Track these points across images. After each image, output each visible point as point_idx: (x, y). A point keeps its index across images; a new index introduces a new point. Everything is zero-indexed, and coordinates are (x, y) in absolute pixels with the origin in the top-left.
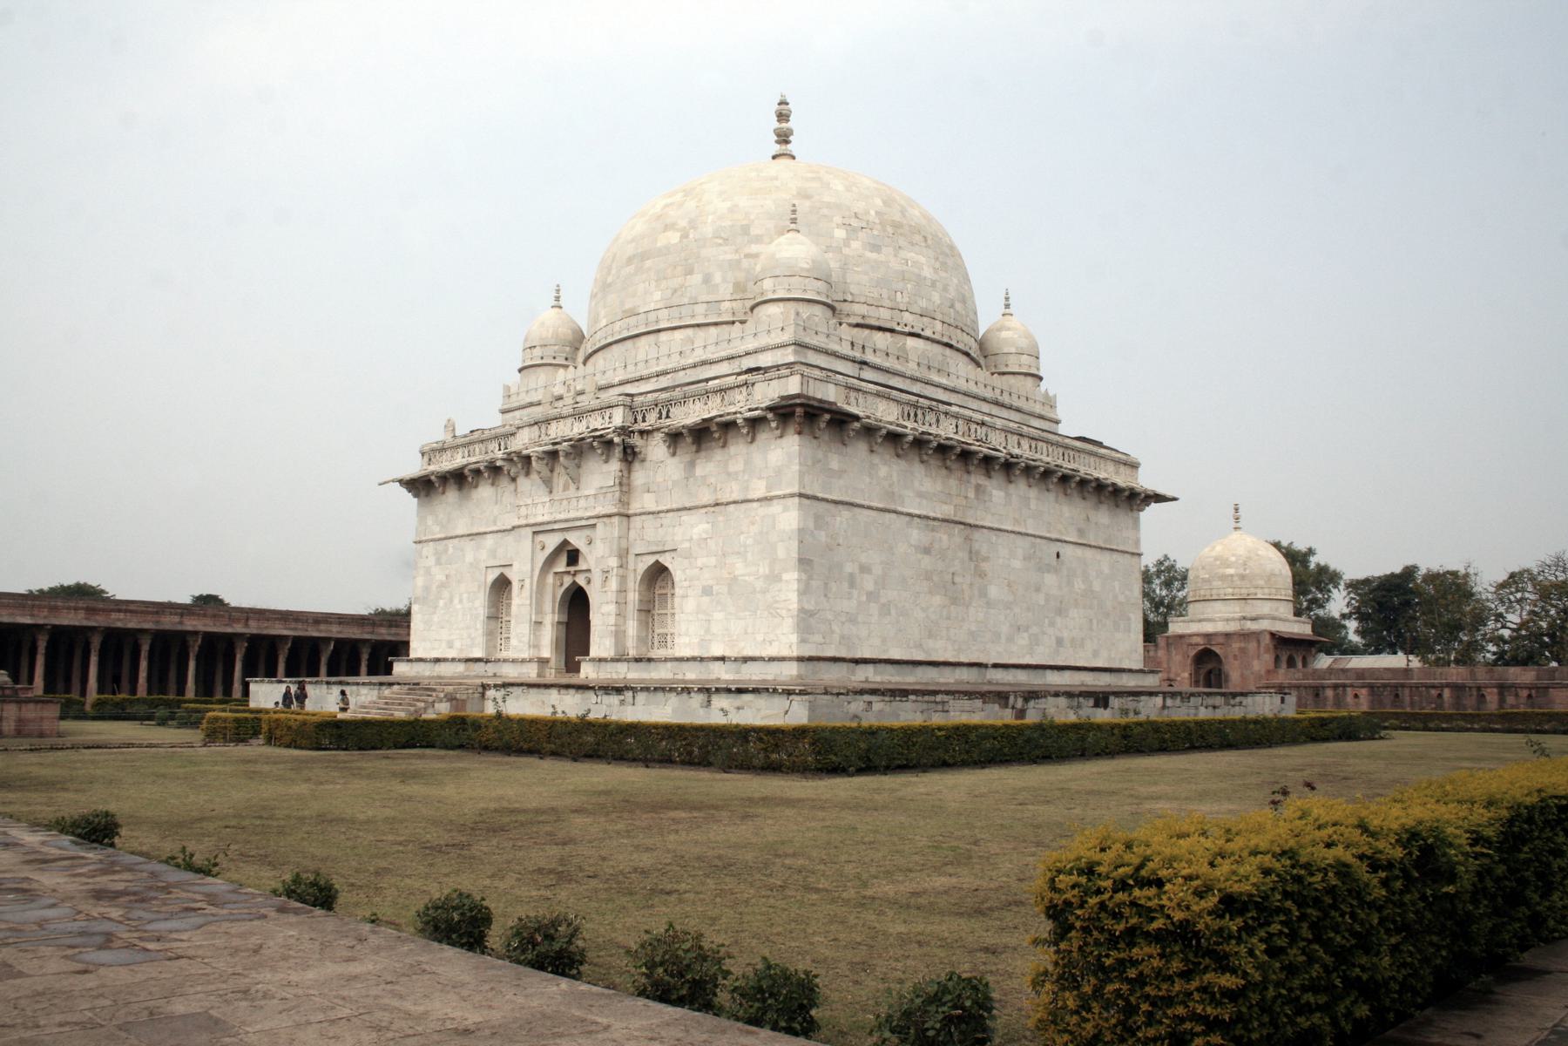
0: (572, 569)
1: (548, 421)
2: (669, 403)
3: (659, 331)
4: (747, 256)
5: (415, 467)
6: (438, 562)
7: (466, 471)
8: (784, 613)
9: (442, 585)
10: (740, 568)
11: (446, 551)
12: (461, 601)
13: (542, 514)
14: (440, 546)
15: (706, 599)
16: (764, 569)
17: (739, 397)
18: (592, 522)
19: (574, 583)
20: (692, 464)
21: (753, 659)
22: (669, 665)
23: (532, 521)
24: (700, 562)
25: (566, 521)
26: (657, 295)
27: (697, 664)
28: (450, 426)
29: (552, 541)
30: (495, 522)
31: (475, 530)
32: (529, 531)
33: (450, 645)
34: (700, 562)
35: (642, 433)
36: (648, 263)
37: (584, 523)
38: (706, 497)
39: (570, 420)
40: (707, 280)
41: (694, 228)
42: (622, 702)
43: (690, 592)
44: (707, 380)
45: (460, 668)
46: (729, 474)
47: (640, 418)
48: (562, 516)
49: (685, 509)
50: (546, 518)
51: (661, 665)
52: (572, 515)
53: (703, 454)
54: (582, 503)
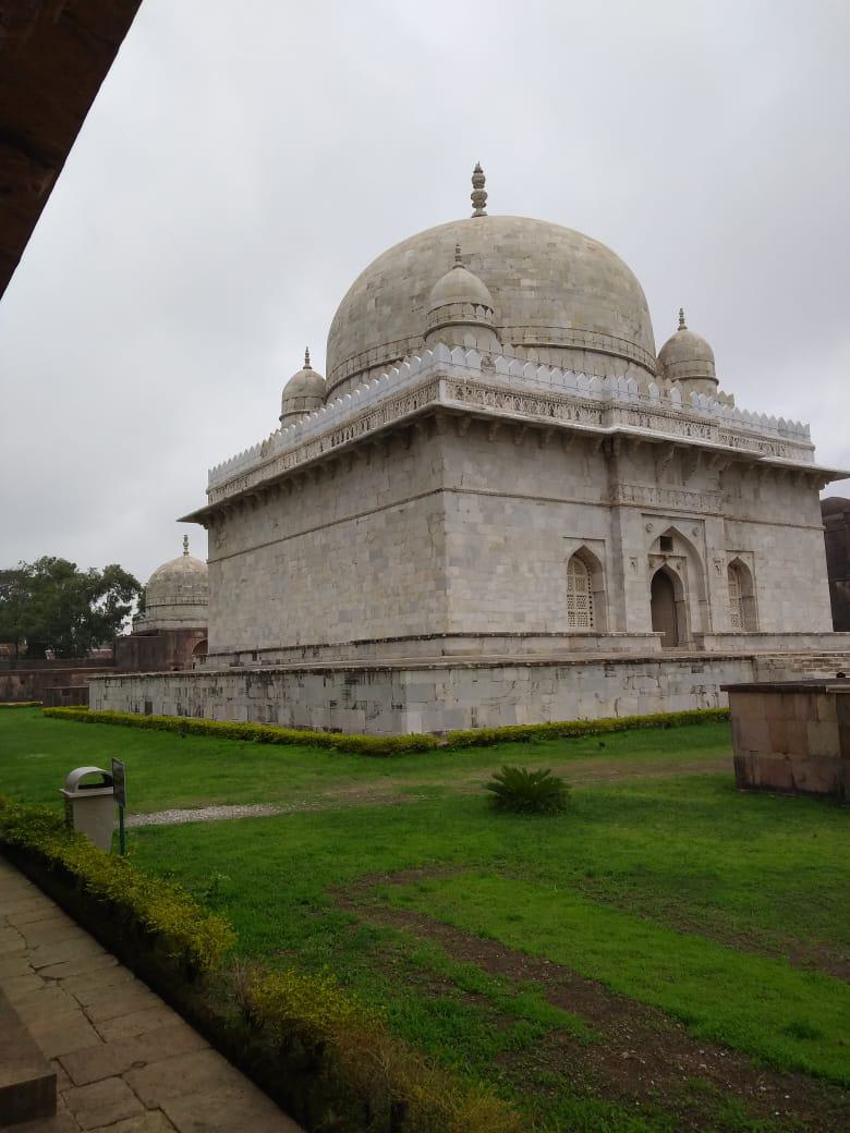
0: (667, 554)
6: (488, 520)
9: (497, 548)
12: (531, 570)
13: (651, 499)
18: (703, 517)
22: (775, 638)
33: (520, 618)
36: (613, 296)
45: (564, 643)
50: (655, 504)
51: (772, 639)
52: (680, 506)
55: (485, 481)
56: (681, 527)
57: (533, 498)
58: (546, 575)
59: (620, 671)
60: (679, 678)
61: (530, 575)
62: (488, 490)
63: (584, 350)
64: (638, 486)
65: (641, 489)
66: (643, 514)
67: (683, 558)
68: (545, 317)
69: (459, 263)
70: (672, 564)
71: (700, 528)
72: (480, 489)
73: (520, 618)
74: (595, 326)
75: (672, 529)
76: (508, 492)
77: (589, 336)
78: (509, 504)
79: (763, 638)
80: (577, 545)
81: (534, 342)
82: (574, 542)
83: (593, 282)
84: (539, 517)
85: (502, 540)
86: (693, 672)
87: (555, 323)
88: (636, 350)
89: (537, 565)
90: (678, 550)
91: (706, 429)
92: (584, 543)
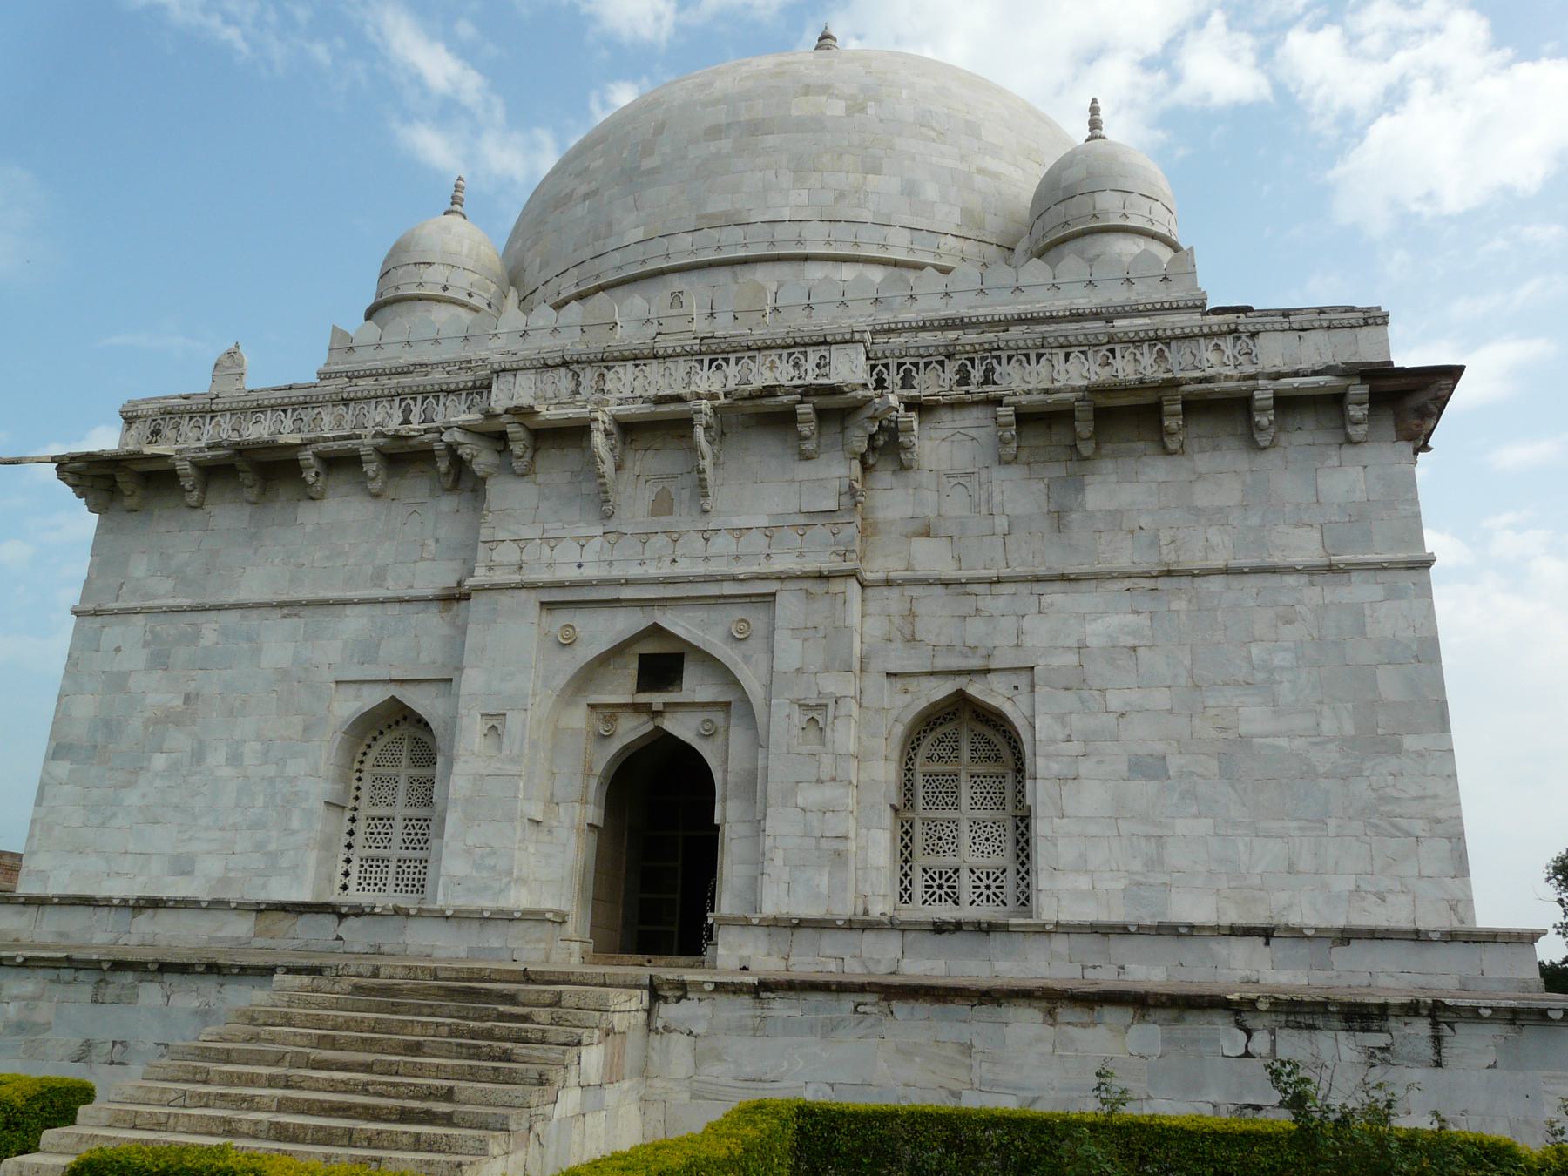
0: (657, 699)
2: (994, 352)
3: (807, 258)
4: (980, 171)
6: (159, 661)
7: (307, 456)
8: (1419, 827)
9: (168, 719)
10: (1253, 718)
11: (197, 636)
12: (234, 759)
14: (170, 628)
15: (1142, 791)
16: (1338, 722)
17: (1213, 357)
19: (658, 728)
20: (1076, 484)
21: (1374, 935)
23: (544, 576)
24: (1115, 701)
27: (1167, 944)
28: (229, 364)
30: (378, 578)
31: (305, 594)
32: (534, 598)
34: (1115, 701)
35: (911, 405)
36: (771, 141)
37: (729, 589)
38: (1125, 557)
39: (681, 366)
40: (910, 190)
41: (879, 101)
42: (1379, 1057)
43: (1085, 767)
45: (241, 927)
46: (1197, 512)
47: (893, 378)
48: (652, 571)
50: (591, 572)
52: (682, 568)
53: (1107, 465)
54: (721, 543)
55: (169, 584)
56: (681, 624)
58: (271, 770)
61: (226, 772)
62: (172, 602)
64: (536, 530)
65: (553, 542)
66: (544, 605)
67: (727, 705)
68: (597, 238)
69: (457, 207)
70: (682, 727)
71: (756, 617)
73: (183, 866)
74: (699, 217)
75: (656, 631)
78: (210, 629)
79: (997, 939)
80: (374, 698)
82: (366, 689)
84: (279, 644)
85: (178, 702)
87: (613, 243)
88: (838, 231)
89: (251, 749)
90: (695, 686)
91: (813, 356)
92: (394, 691)
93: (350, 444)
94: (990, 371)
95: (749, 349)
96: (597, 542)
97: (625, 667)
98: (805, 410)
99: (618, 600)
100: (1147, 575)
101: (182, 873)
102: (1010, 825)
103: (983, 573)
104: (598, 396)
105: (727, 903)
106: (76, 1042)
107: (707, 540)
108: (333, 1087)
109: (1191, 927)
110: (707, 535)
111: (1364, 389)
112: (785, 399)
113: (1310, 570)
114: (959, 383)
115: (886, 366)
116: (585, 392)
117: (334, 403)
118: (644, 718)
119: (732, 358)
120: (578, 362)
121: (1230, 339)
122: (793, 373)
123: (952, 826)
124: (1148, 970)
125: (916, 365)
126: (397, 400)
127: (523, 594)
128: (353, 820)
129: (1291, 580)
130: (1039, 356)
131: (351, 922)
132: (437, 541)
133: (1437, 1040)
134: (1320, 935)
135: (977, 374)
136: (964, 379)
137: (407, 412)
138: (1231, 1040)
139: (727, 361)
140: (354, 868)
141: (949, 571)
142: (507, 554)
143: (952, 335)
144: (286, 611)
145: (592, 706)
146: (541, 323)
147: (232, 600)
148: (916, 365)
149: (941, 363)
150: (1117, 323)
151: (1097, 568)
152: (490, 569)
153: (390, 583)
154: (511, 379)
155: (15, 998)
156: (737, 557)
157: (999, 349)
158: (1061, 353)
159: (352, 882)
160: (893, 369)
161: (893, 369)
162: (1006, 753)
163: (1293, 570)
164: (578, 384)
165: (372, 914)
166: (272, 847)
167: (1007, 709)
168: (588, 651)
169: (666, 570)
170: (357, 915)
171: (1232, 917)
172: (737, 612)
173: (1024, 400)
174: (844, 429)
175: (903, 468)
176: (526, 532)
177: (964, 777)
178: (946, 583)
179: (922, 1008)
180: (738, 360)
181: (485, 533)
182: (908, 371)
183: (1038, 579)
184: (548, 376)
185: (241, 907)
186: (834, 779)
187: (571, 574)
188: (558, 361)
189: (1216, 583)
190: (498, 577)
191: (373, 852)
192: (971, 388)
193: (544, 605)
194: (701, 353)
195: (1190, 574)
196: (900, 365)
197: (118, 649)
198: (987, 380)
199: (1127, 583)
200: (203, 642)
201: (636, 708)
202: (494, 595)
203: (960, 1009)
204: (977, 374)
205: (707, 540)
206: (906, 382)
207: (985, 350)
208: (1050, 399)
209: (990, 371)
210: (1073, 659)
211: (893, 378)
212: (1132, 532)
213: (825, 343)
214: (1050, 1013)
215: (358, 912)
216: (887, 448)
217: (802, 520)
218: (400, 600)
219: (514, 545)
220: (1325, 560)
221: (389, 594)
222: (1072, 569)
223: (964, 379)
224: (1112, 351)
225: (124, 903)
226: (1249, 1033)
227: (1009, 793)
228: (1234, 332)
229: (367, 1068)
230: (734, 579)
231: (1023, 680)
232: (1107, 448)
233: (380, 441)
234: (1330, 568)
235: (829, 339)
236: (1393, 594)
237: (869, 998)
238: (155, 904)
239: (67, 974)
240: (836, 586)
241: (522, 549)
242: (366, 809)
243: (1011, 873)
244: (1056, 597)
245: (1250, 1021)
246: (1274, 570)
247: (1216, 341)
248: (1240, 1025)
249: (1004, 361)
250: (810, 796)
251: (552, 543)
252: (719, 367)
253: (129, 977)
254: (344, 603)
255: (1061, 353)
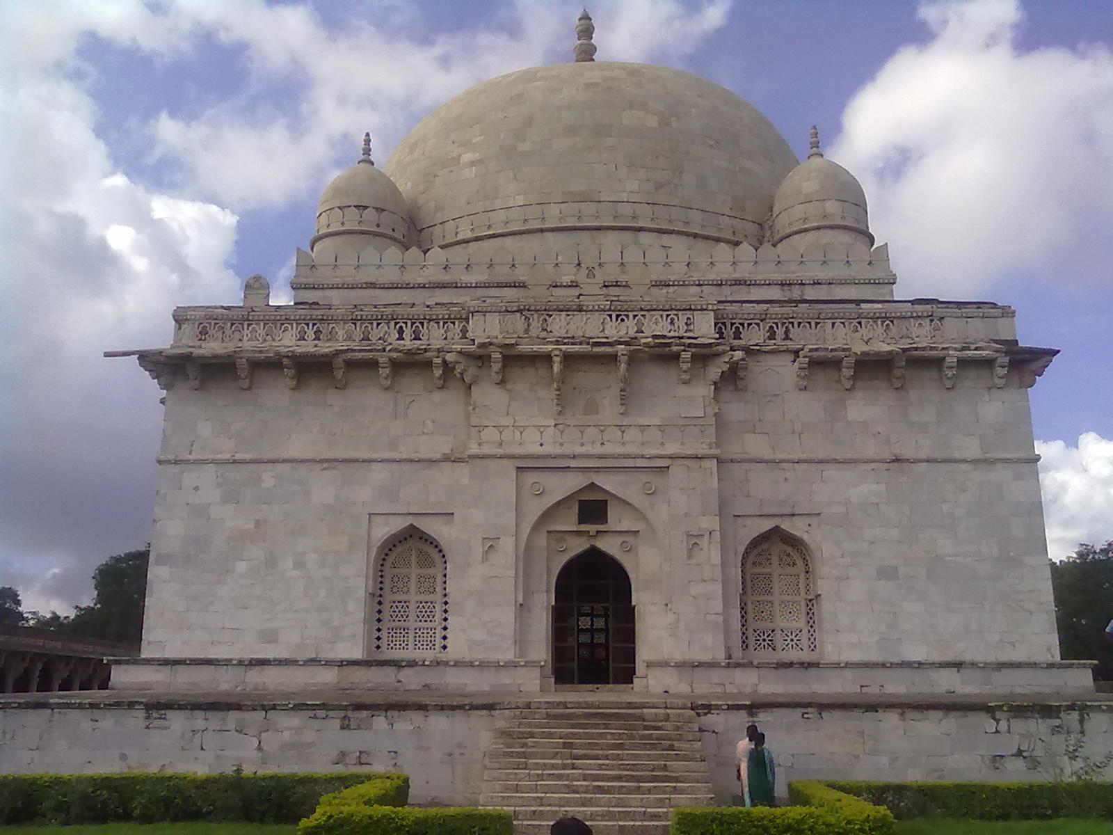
0: (592, 528)
1: (548, 311)
2: (788, 322)
3: (641, 229)
5: (163, 339)
12: (299, 564)
14: (238, 474)
17: (915, 331)
25: (601, 457)
26: (633, 185)
27: (907, 671)
29: (563, 486)
30: (393, 444)
31: (340, 454)
32: (510, 466)
44: (858, 302)
47: (730, 332)
49: (836, 461)
50: (548, 449)
52: (609, 449)
53: (859, 394)
54: (632, 434)
56: (609, 483)
57: (314, 461)
59: (177, 720)
60: (309, 736)
61: (296, 573)
63: (542, 231)
65: (522, 429)
66: (519, 469)
70: (609, 546)
72: (219, 456)
73: (270, 637)
76: (266, 456)
77: (554, 210)
78: (268, 478)
79: (812, 670)
81: (469, 235)
82: (392, 519)
83: (571, 130)
84: (323, 489)
85: (251, 525)
86: (342, 728)
87: (499, 203)
89: (311, 559)
90: (617, 520)
91: (683, 318)
93: (371, 355)
94: (787, 332)
95: (642, 310)
96: (551, 430)
97: (570, 508)
98: (686, 355)
99: (569, 467)
100: (882, 461)
101: (269, 642)
102: (803, 603)
103: (791, 457)
104: (544, 334)
105: (643, 654)
106: (334, 754)
107: (623, 432)
108: (600, 767)
109: (920, 663)
110: (623, 428)
111: (1007, 359)
112: (675, 349)
113: (972, 462)
114: (770, 338)
115: (724, 324)
116: (535, 331)
117: (345, 321)
118: (584, 539)
119: (631, 315)
120: (528, 310)
121: (928, 320)
122: (669, 327)
123: (770, 604)
124: (897, 686)
125: (742, 324)
126: (392, 323)
127: (505, 462)
128: (380, 603)
129: (964, 467)
130: (817, 324)
131: (407, 671)
132: (434, 422)
133: (1082, 721)
134: (986, 666)
135: (780, 332)
136: (772, 336)
137: (401, 331)
138: (990, 725)
139: (627, 316)
140: (384, 634)
141: (767, 453)
142: (490, 434)
143: (765, 306)
144: (326, 465)
145: (548, 532)
146: (458, 260)
147: (285, 457)
148: (742, 324)
149: (758, 324)
150: (863, 306)
151: (856, 456)
152: (479, 444)
153: (402, 449)
154: (482, 317)
155: (288, 729)
156: (643, 444)
157: (793, 318)
158: (830, 322)
159: (383, 643)
160: (729, 327)
161: (729, 327)
162: (800, 562)
163: (964, 461)
164: (529, 325)
165: (424, 665)
166: (336, 623)
167: (806, 537)
168: (549, 501)
169: (598, 450)
170: (411, 666)
171: (936, 657)
172: (644, 477)
173: (815, 354)
174: (705, 366)
175: (737, 389)
176: (504, 421)
177: (775, 575)
178: (767, 462)
179: (837, 714)
180: (635, 316)
181: (474, 420)
182: (737, 328)
183: (821, 462)
184: (509, 316)
185: (329, 663)
186: (712, 580)
187: (537, 450)
188: (515, 309)
189: (922, 467)
190: (486, 450)
191: (397, 623)
192: (778, 342)
193: (519, 469)
194: (610, 310)
195: (908, 460)
196: (732, 324)
197: (196, 488)
198: (787, 338)
199: (873, 465)
200: (264, 485)
201: (578, 533)
202: (486, 462)
203: (857, 713)
204: (780, 332)
205: (623, 432)
206: (737, 336)
207: (786, 319)
208: (830, 355)
209: (787, 332)
210: (842, 509)
211: (730, 332)
212: (874, 435)
213: (690, 309)
214: (902, 714)
215: (412, 664)
216: (733, 378)
217: (682, 422)
218: (412, 461)
219: (495, 429)
220: (982, 456)
221: (404, 456)
222: (839, 455)
223: (772, 336)
224: (860, 323)
225: (240, 663)
226: (998, 721)
227: (802, 585)
228: (931, 317)
229: (607, 757)
230: (643, 457)
231: (813, 521)
232: (859, 384)
233: (394, 355)
234: (985, 461)
235: (693, 307)
236: (1018, 477)
237: (809, 710)
238: (263, 663)
239: (321, 713)
240: (706, 464)
241: (501, 433)
242: (388, 597)
243: (805, 631)
244: (830, 472)
245: (998, 715)
246: (955, 461)
247: (920, 321)
248: (994, 718)
249: (796, 325)
250: (696, 589)
251: (522, 429)
252: (623, 320)
253: (364, 714)
254: (371, 461)
255: (830, 322)
